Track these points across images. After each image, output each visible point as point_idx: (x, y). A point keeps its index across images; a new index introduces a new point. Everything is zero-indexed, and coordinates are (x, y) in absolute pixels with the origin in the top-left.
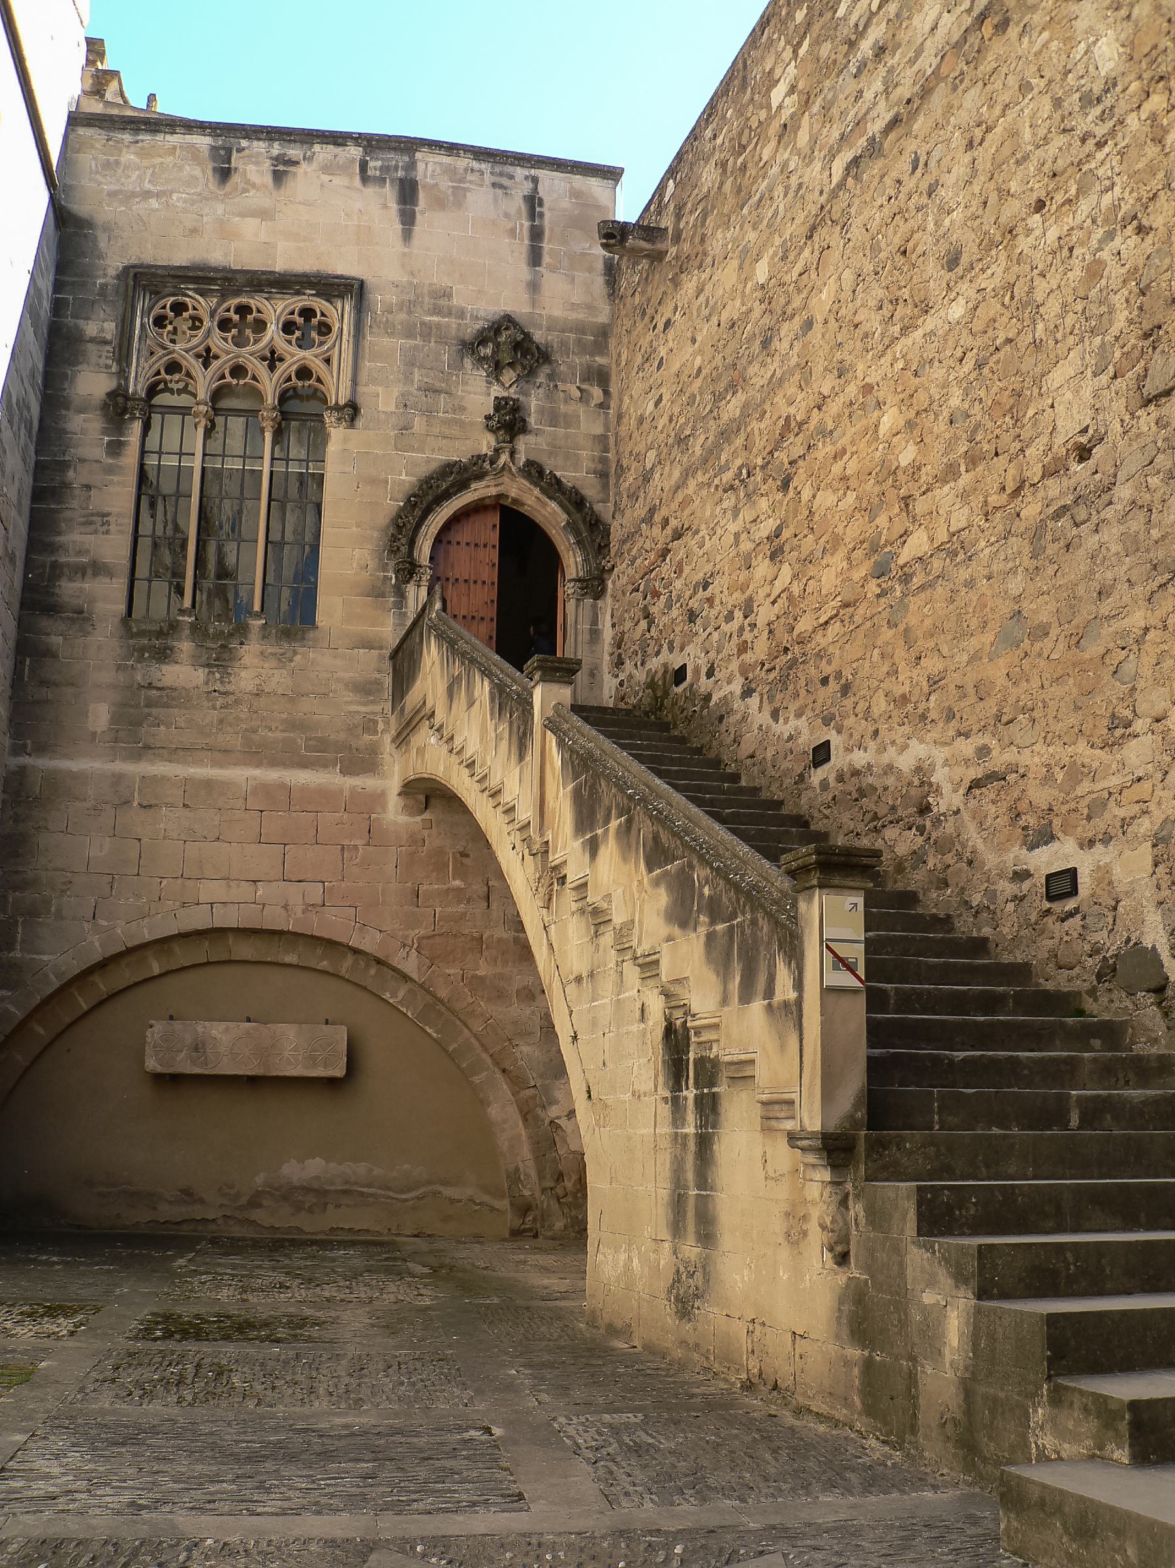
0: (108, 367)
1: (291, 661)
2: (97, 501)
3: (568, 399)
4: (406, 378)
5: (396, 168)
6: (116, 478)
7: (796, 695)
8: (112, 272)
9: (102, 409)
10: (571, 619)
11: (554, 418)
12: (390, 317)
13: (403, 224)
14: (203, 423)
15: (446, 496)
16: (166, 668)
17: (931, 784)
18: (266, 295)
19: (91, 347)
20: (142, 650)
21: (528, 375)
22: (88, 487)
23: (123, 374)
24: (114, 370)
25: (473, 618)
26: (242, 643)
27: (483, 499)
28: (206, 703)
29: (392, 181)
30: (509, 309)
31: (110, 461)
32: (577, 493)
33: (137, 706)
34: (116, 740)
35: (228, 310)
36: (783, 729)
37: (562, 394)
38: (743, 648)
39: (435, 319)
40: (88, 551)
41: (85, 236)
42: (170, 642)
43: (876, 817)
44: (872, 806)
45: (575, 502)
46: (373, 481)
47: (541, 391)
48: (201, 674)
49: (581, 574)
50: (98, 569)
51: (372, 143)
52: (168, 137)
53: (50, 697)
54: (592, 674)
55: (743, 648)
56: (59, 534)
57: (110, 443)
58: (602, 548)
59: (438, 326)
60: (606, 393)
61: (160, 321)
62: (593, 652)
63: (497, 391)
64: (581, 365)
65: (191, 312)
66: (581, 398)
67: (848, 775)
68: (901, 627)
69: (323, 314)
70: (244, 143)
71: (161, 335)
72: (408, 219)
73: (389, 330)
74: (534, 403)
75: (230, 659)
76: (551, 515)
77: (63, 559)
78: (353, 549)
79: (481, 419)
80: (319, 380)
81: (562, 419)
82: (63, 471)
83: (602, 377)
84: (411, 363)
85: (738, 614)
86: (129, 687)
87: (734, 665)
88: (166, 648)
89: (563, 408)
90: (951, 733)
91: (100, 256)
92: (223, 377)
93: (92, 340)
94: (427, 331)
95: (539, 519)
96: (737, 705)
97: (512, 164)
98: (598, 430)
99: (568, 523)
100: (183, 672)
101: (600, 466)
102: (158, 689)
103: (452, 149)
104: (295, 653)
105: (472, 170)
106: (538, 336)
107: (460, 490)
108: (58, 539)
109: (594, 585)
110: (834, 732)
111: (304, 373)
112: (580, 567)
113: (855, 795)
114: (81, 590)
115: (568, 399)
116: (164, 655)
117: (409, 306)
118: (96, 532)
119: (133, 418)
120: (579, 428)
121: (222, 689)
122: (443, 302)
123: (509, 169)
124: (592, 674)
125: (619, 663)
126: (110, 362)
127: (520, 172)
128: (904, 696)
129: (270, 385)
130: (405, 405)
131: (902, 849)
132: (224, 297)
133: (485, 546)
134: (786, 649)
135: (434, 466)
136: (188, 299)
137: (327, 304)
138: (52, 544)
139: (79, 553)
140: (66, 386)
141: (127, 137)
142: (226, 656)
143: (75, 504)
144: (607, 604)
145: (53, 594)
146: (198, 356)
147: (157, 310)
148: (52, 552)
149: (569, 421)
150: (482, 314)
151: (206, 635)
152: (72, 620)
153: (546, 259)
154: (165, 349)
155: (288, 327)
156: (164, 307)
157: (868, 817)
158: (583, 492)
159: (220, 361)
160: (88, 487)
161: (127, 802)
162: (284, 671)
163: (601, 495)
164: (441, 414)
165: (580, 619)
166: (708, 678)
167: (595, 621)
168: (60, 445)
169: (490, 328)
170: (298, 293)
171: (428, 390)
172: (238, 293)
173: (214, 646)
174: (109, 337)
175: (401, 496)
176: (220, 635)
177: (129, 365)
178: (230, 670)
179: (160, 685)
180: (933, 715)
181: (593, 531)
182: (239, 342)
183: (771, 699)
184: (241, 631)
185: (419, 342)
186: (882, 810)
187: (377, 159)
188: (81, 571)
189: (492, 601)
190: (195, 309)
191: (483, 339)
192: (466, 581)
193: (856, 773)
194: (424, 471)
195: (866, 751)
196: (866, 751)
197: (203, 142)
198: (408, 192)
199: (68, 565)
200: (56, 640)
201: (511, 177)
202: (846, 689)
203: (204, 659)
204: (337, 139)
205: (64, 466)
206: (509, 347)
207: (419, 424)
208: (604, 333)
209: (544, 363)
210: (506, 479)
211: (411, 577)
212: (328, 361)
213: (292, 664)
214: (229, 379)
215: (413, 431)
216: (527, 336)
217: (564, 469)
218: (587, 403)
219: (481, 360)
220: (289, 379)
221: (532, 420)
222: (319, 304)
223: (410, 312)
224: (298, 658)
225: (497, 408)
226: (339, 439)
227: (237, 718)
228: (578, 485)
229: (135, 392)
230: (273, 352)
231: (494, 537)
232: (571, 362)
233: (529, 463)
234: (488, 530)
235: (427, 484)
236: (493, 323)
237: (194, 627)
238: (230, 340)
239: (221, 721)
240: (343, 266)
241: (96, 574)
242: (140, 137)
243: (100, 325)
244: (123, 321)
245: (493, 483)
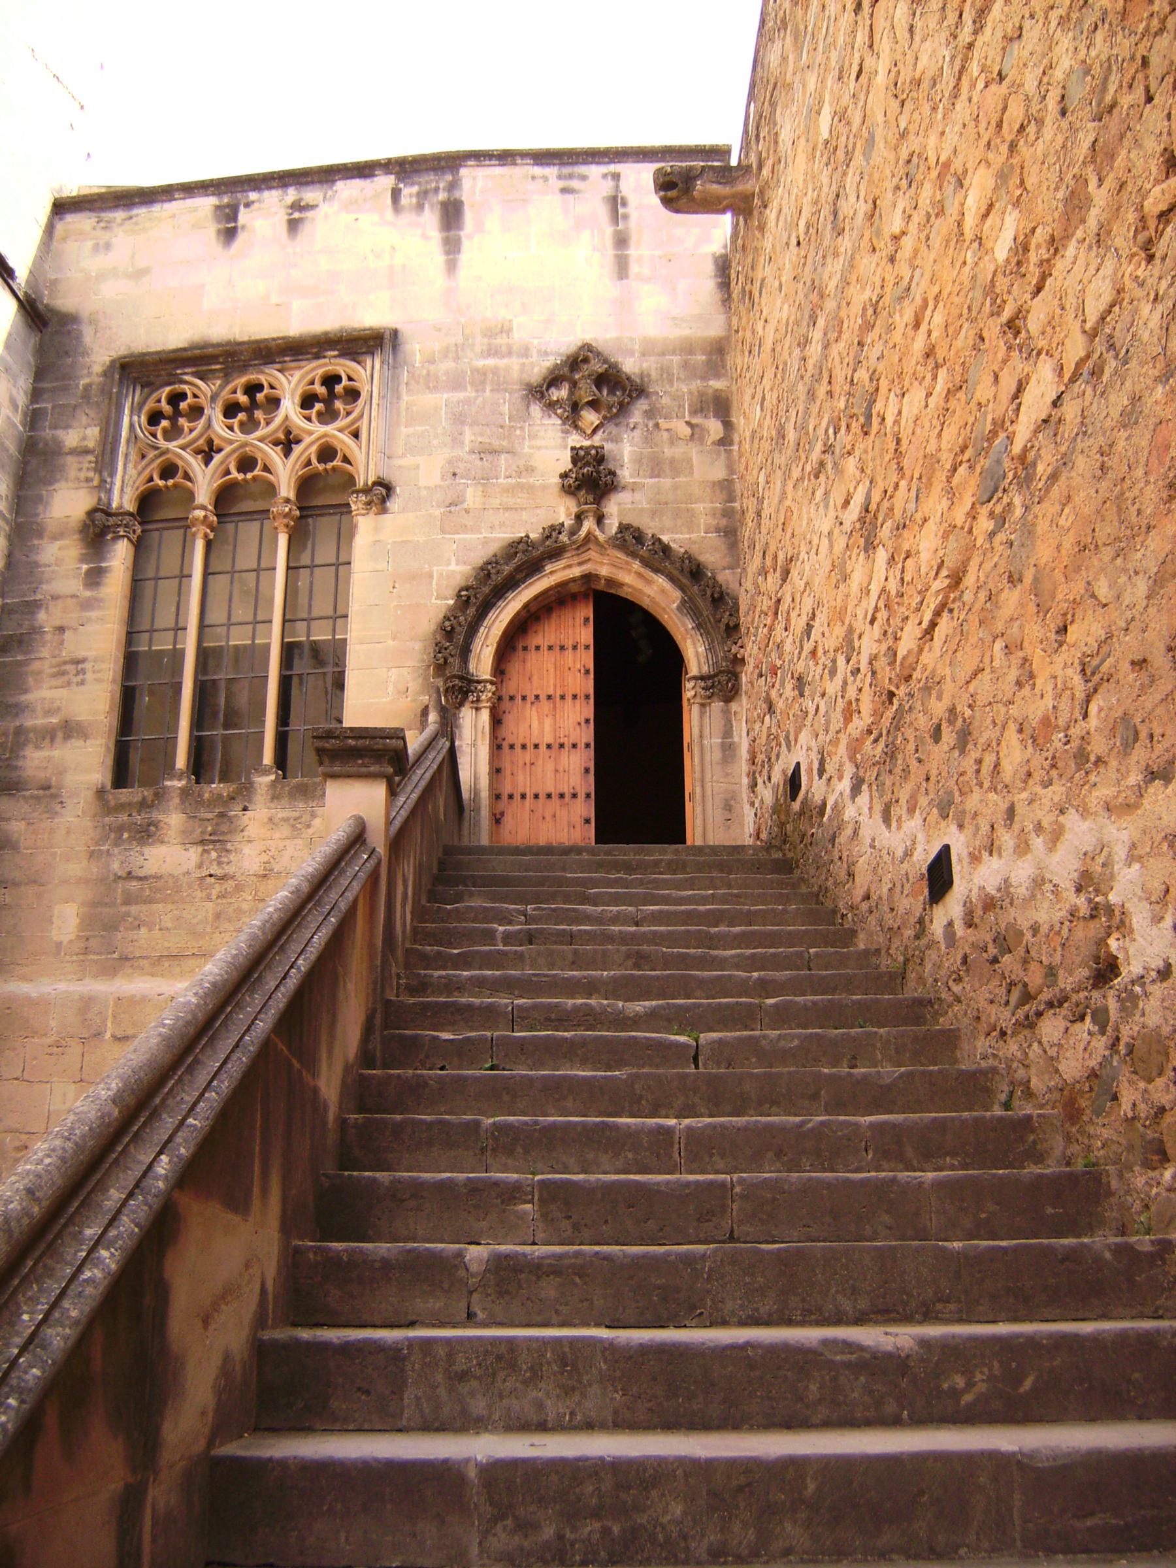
0: (88, 480)
1: (308, 826)
2: (73, 645)
3: (674, 440)
4: (454, 440)
5: (437, 190)
6: (93, 614)
7: (906, 771)
8: (98, 369)
9: (81, 532)
10: (696, 731)
11: (656, 466)
12: (432, 368)
13: (447, 253)
14: (201, 535)
15: (511, 583)
16: (148, 851)
17: (1109, 910)
18: (278, 366)
19: (71, 460)
20: (120, 829)
21: (616, 415)
22: (61, 629)
23: (104, 486)
24: (96, 483)
25: (562, 746)
26: (245, 809)
27: (563, 585)
28: (198, 894)
29: (432, 206)
30: (588, 337)
31: (88, 594)
32: (690, 558)
33: (113, 904)
34: (86, 951)
35: (235, 392)
36: (893, 840)
37: (666, 435)
38: (849, 713)
39: (491, 362)
40: (59, 709)
41: (69, 332)
42: (156, 815)
43: (1027, 997)
44: (1018, 973)
45: (690, 573)
46: (414, 577)
47: (637, 433)
48: (193, 855)
49: (705, 669)
50: (70, 730)
51: (404, 168)
52: (167, 206)
53: (8, 900)
54: (728, 807)
55: (849, 713)
56: (26, 691)
57: (89, 573)
58: (732, 630)
59: (495, 371)
60: (728, 425)
61: (154, 418)
62: (727, 775)
63: (576, 440)
64: (690, 393)
65: (190, 400)
66: (693, 434)
67: (979, 912)
68: (1028, 578)
69: (350, 379)
70: (253, 196)
71: (154, 436)
72: (452, 247)
73: (432, 383)
74: (625, 450)
75: (230, 832)
76: (658, 594)
77: (29, 723)
78: (389, 669)
79: (556, 480)
80: (346, 460)
81: (666, 467)
82: (33, 613)
83: (721, 407)
84: (459, 419)
85: (841, 660)
86: (102, 880)
87: (842, 750)
88: (149, 825)
89: (668, 452)
90: (1134, 778)
91: (85, 353)
92: (228, 472)
93: (74, 452)
94: (481, 378)
95: (645, 603)
96: (849, 813)
97: (585, 163)
98: (719, 473)
99: (683, 602)
100: (171, 855)
101: (724, 522)
102: (141, 879)
103: (506, 157)
104: (313, 816)
105: (533, 178)
106: (630, 366)
107: (530, 575)
108: (23, 698)
109: (724, 683)
110: (954, 828)
111: (327, 453)
112: (703, 660)
113: (993, 951)
114: (49, 759)
115: (674, 440)
116: (146, 834)
117: (455, 352)
118: (69, 683)
119: (117, 538)
120: (691, 473)
121: (219, 872)
122: (501, 340)
123: (582, 169)
124: (728, 807)
125: (753, 786)
126: (91, 474)
127: (595, 171)
128: (1046, 722)
129: (285, 474)
130: (454, 474)
131: (1072, 1068)
132: (227, 376)
133: (575, 648)
134: (891, 695)
135: (494, 548)
136: (186, 387)
137: (354, 365)
138: (16, 705)
139: (49, 712)
140: (41, 508)
141: (119, 215)
142: (224, 828)
143: (45, 652)
144: (742, 707)
145: (16, 768)
146: (198, 452)
147: (150, 405)
148: (17, 715)
149: (677, 467)
150: (552, 347)
151: (200, 803)
152: (37, 798)
153: (634, 269)
154: (158, 448)
155: (307, 401)
156: (159, 401)
157: (1015, 996)
158: (702, 558)
159: (223, 453)
160: (61, 629)
161: (98, 1035)
162: (299, 841)
163: (728, 559)
164: (501, 481)
165: (707, 731)
166: (820, 777)
167: (728, 733)
168: (30, 583)
169: (564, 363)
170: (317, 357)
171: (486, 451)
172: (244, 368)
173: (210, 816)
174: (91, 444)
175: (452, 592)
176: (217, 799)
177: (112, 474)
178: (229, 846)
179: (141, 873)
180: (1098, 746)
181: (716, 607)
182: (249, 426)
183: (881, 786)
184: (245, 792)
185: (470, 393)
186: (1035, 978)
187: (413, 184)
188: (49, 735)
189: (587, 721)
190: (195, 396)
191: (553, 380)
192: (549, 697)
193: (990, 904)
194: (480, 556)
195: (1000, 856)
196: (1000, 856)
197: (206, 203)
198: (452, 214)
199: (34, 729)
200: (17, 827)
201: (584, 178)
202: (964, 738)
203: (197, 835)
204: (363, 170)
205: (32, 607)
206: (591, 385)
207: (472, 497)
208: (718, 351)
209: (638, 397)
210: (592, 554)
211: (465, 697)
212: (356, 435)
213: (310, 831)
214: (235, 475)
215: (465, 506)
216: (614, 366)
217: (673, 531)
218: (702, 440)
219: (551, 406)
220: (309, 463)
221: (626, 475)
222: (343, 366)
223: (457, 358)
224: (317, 822)
225: (575, 460)
226: (368, 530)
227: (238, 910)
228: (695, 550)
229: (121, 507)
230: (288, 433)
231: (586, 635)
232: (676, 392)
233: (623, 528)
234: (578, 628)
235: (485, 572)
236: (568, 357)
237: (185, 793)
238: (236, 428)
239: (218, 916)
240: (369, 318)
241: (67, 737)
242: (135, 211)
243: (81, 433)
244: (107, 423)
245: (576, 560)
